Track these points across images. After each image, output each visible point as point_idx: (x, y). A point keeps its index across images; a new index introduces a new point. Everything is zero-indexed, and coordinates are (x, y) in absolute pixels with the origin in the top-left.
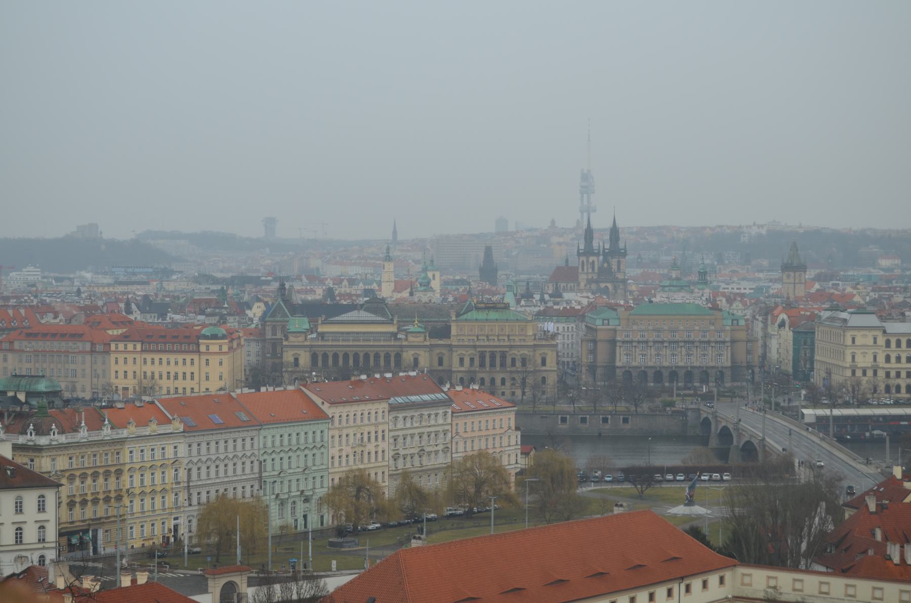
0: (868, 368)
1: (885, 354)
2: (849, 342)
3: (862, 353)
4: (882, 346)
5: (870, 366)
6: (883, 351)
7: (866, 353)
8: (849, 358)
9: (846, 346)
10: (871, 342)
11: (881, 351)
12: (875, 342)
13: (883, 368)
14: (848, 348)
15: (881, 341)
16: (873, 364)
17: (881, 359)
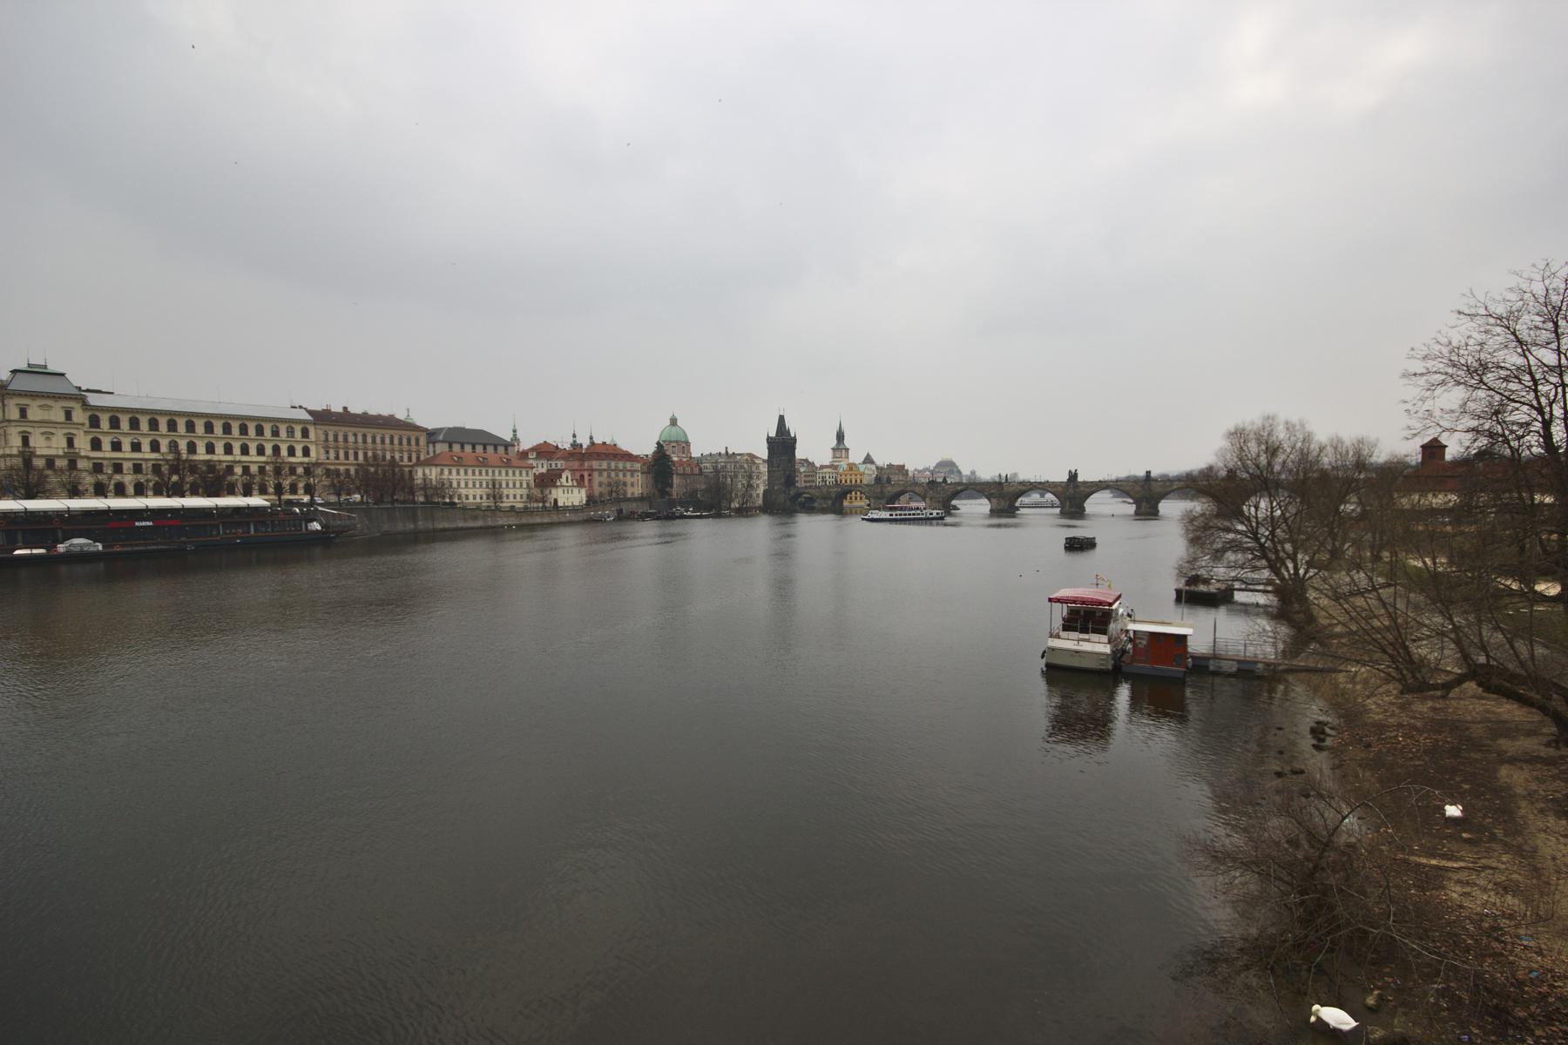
0: (59, 457)
1: (90, 437)
2: (14, 414)
3: (43, 434)
4: (83, 424)
5: (61, 453)
6: (85, 432)
7: (53, 434)
8: (16, 442)
9: (9, 421)
10: (61, 417)
11: (82, 433)
12: (68, 415)
13: (88, 458)
14: (13, 424)
15: (79, 416)
16: (66, 450)
17: (82, 444)
